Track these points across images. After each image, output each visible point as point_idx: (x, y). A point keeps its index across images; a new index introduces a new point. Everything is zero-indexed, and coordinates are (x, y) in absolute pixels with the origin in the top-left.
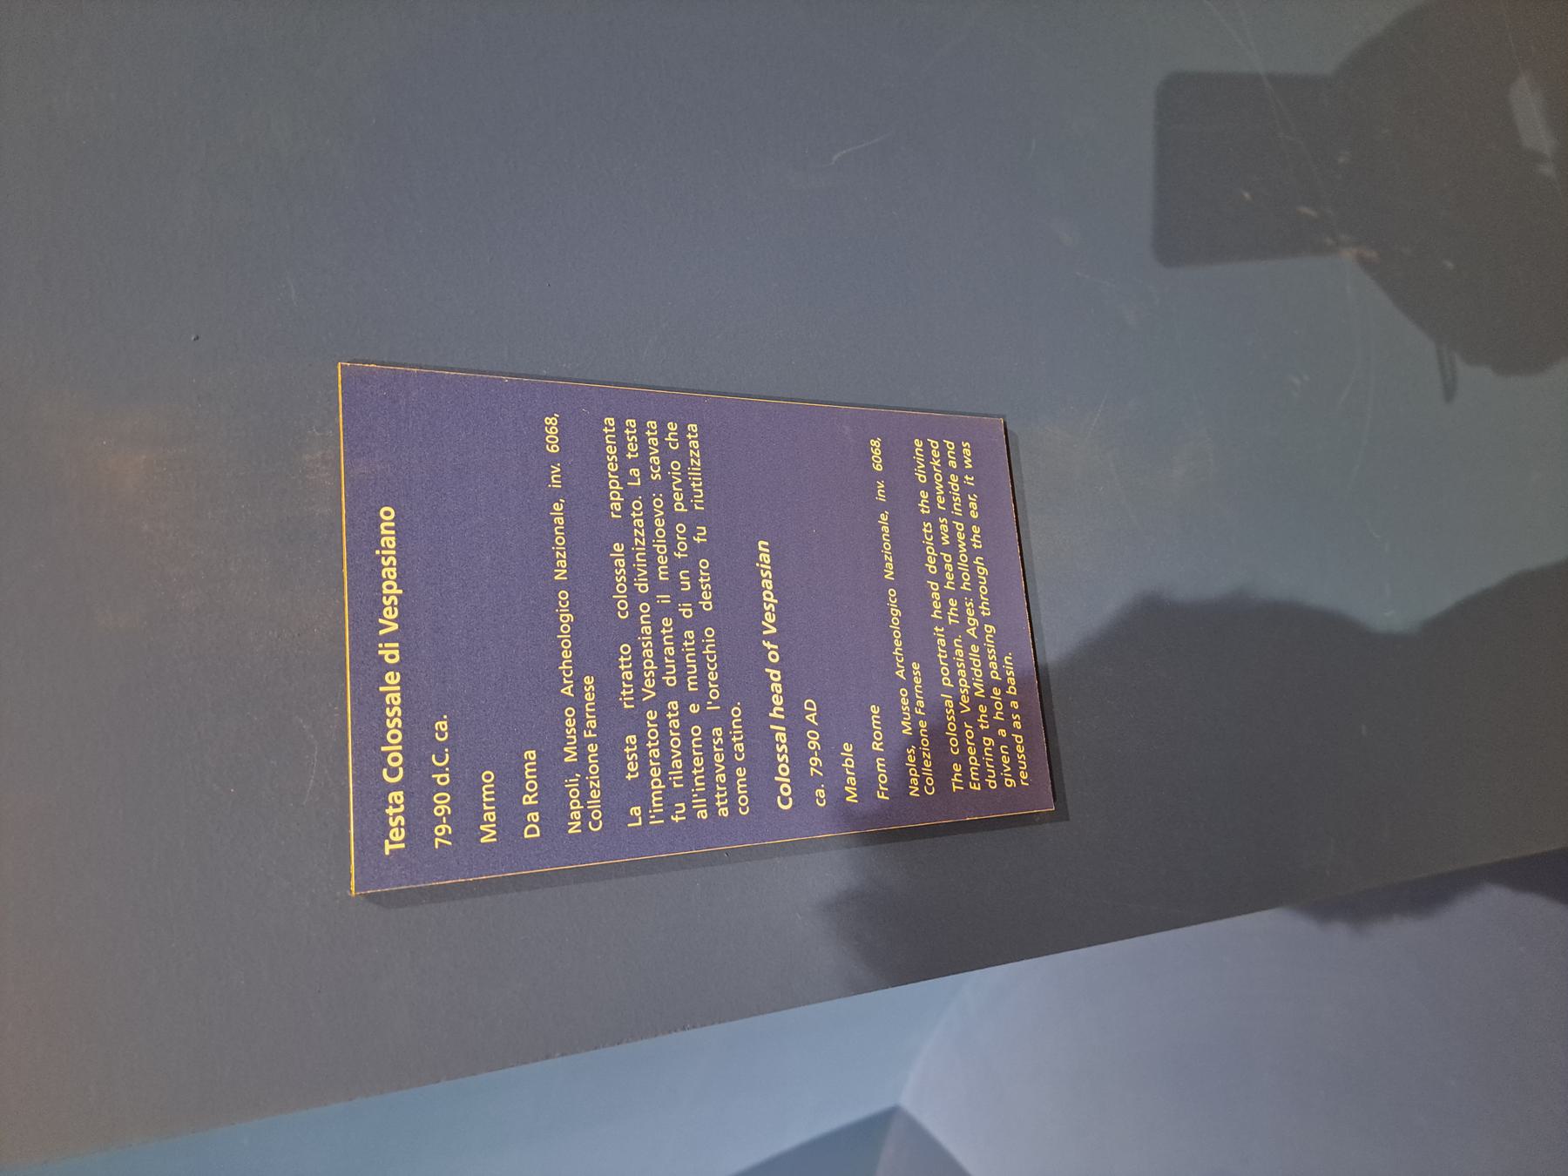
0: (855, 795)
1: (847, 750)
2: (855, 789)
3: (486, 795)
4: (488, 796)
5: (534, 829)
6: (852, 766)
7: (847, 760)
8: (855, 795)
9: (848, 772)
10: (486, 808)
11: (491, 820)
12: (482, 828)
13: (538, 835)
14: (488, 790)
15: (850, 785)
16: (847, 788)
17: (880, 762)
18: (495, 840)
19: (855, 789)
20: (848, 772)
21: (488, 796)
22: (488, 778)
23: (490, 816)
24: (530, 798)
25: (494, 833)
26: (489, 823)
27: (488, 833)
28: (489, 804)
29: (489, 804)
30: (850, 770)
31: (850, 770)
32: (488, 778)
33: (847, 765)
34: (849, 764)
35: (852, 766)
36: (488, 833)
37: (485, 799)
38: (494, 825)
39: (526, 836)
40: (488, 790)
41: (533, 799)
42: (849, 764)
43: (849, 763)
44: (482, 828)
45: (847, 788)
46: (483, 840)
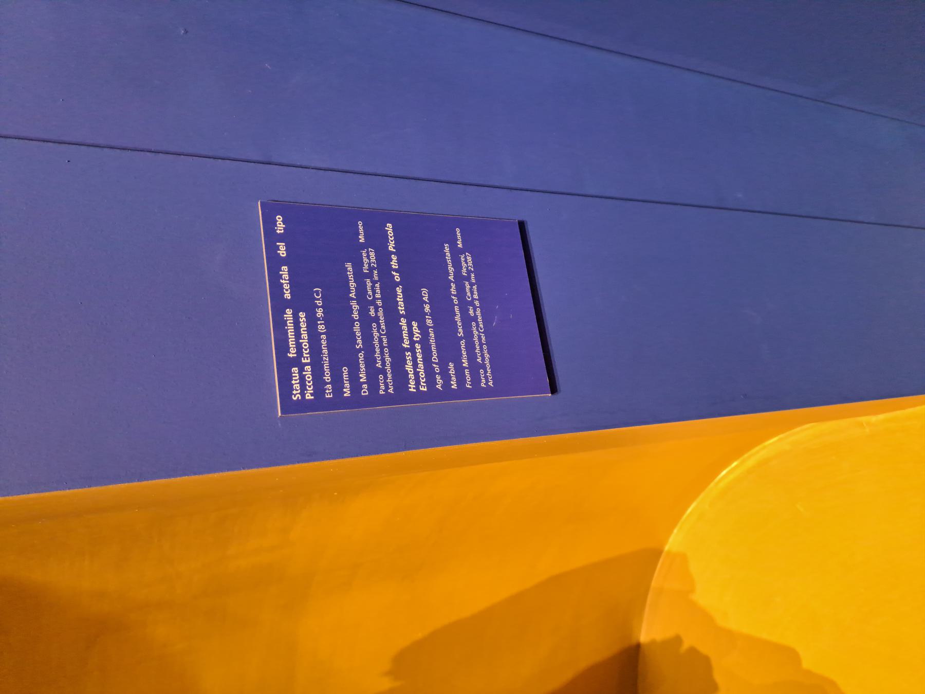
1: (451, 366)
3: (345, 376)
4: (345, 377)
6: (454, 373)
9: (452, 375)
10: (345, 382)
12: (345, 390)
14: (345, 375)
15: (453, 381)
18: (349, 395)
20: (452, 375)
21: (345, 377)
22: (345, 370)
23: (347, 385)
28: (346, 380)
29: (346, 380)
30: (453, 374)
31: (453, 374)
32: (345, 370)
34: (452, 372)
35: (454, 373)
40: (345, 375)
42: (452, 372)
43: (453, 371)
44: (345, 390)
45: (452, 382)
46: (345, 395)
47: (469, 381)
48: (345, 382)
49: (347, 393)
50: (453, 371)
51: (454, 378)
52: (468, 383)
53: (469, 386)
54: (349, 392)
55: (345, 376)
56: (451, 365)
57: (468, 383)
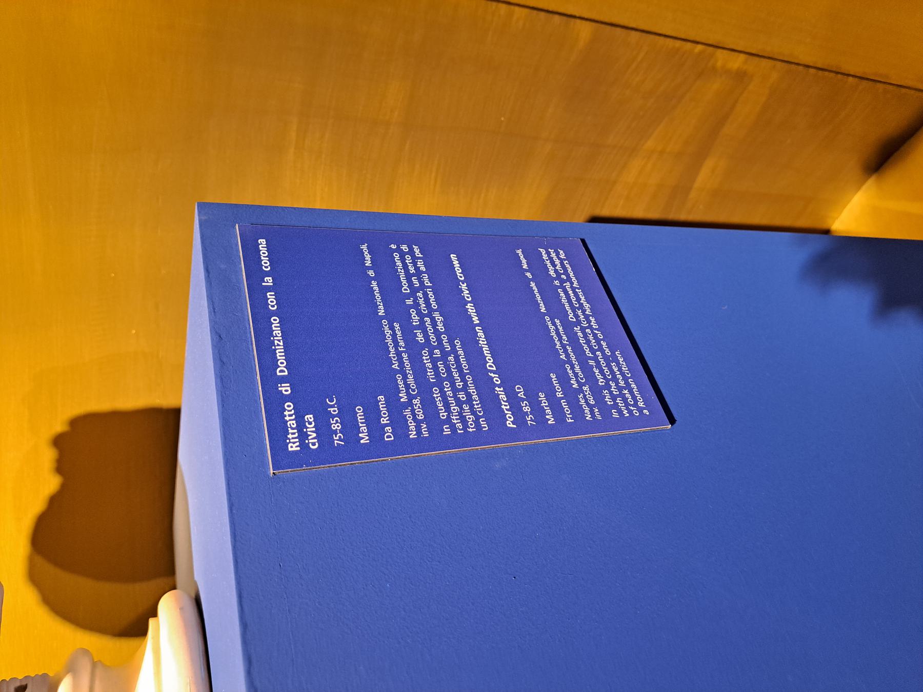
0: (553, 419)
1: (542, 396)
2: (552, 416)
3: (360, 417)
4: (360, 419)
5: (391, 436)
6: (547, 404)
7: (543, 401)
8: (553, 419)
9: (545, 408)
10: (361, 425)
11: (365, 431)
12: (360, 435)
13: (393, 439)
15: (549, 415)
16: (547, 417)
17: (563, 402)
19: (552, 416)
20: (545, 408)
21: (360, 419)
22: (359, 410)
23: (363, 428)
24: (385, 420)
25: (367, 438)
26: (363, 432)
27: (364, 438)
28: (362, 423)
29: (362, 423)
32: (359, 410)
33: (544, 404)
34: (544, 404)
35: (547, 404)
36: (364, 438)
37: (360, 421)
38: (367, 434)
39: (386, 439)
41: (387, 420)
42: (544, 404)
44: (360, 435)
45: (547, 417)
46: (362, 441)
48: (361, 425)
49: (365, 439)
51: (548, 411)
54: (367, 438)
55: (359, 417)
56: (542, 395)
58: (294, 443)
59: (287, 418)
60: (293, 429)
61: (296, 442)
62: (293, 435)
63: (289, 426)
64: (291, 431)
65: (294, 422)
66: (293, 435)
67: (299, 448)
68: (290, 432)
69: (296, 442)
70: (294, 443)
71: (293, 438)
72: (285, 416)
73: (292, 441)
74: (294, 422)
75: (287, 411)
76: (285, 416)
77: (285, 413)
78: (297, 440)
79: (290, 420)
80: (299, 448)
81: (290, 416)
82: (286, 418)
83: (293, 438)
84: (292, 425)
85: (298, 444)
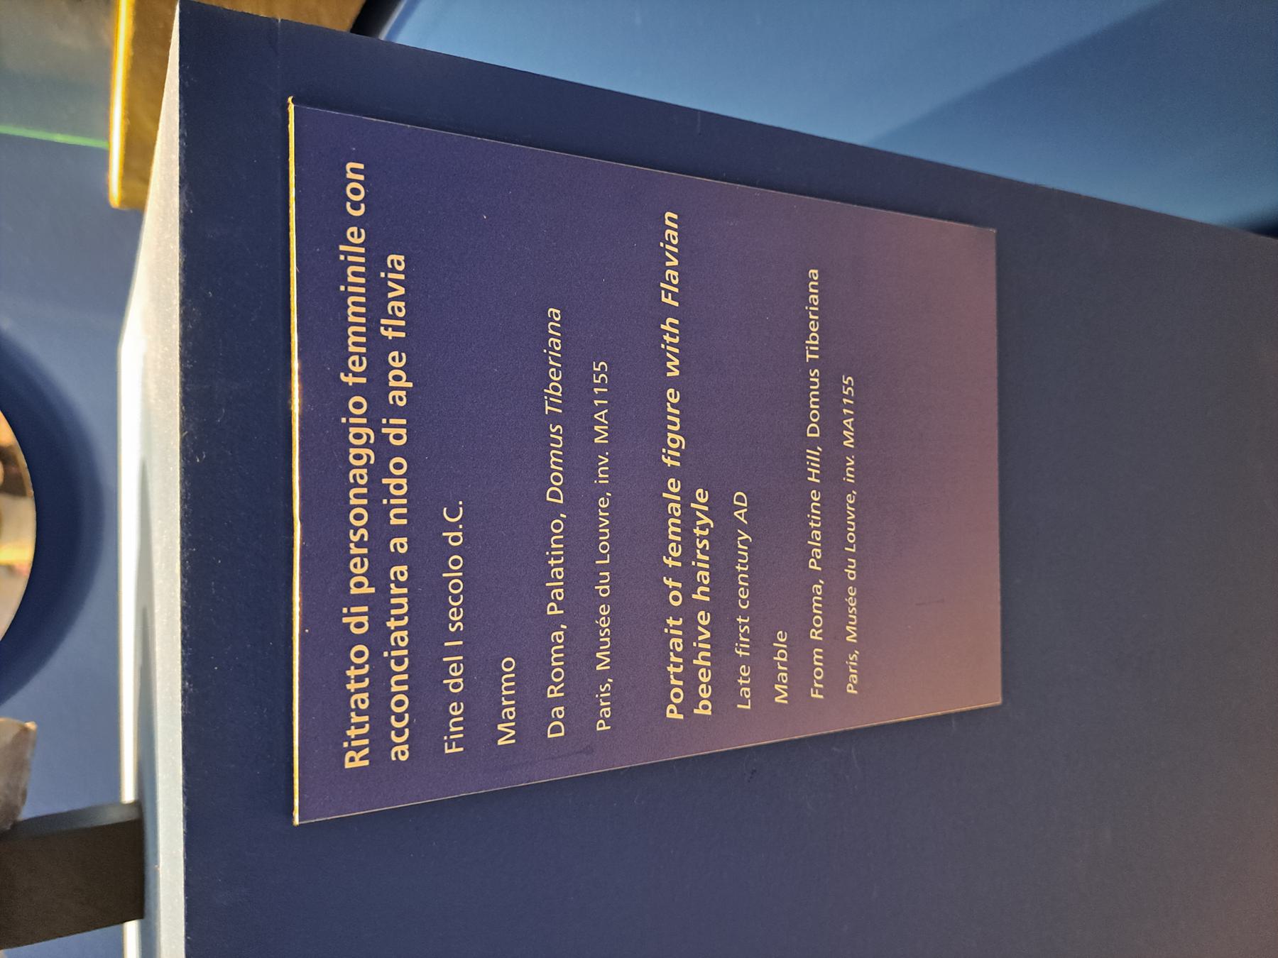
2: (786, 687)
9: (780, 667)
16: (777, 687)
20: (780, 667)
30: (783, 664)
31: (783, 664)
33: (779, 658)
35: (785, 659)
43: (782, 655)
47: (818, 682)
50: (782, 655)
52: (816, 685)
53: (817, 696)
56: (782, 637)
57: (816, 685)
58: (358, 749)
59: (352, 686)
60: (360, 713)
61: (364, 747)
62: (358, 730)
63: (353, 706)
64: (355, 719)
65: (365, 696)
66: (358, 730)
67: (366, 763)
68: (353, 721)
69: (364, 747)
70: (358, 749)
71: (358, 737)
72: (348, 679)
73: (354, 743)
74: (365, 696)
75: (352, 668)
76: (348, 679)
77: (348, 673)
78: (366, 742)
79: (358, 691)
80: (366, 763)
81: (359, 679)
82: (348, 686)
83: (358, 737)
84: (359, 703)
85: (366, 751)
